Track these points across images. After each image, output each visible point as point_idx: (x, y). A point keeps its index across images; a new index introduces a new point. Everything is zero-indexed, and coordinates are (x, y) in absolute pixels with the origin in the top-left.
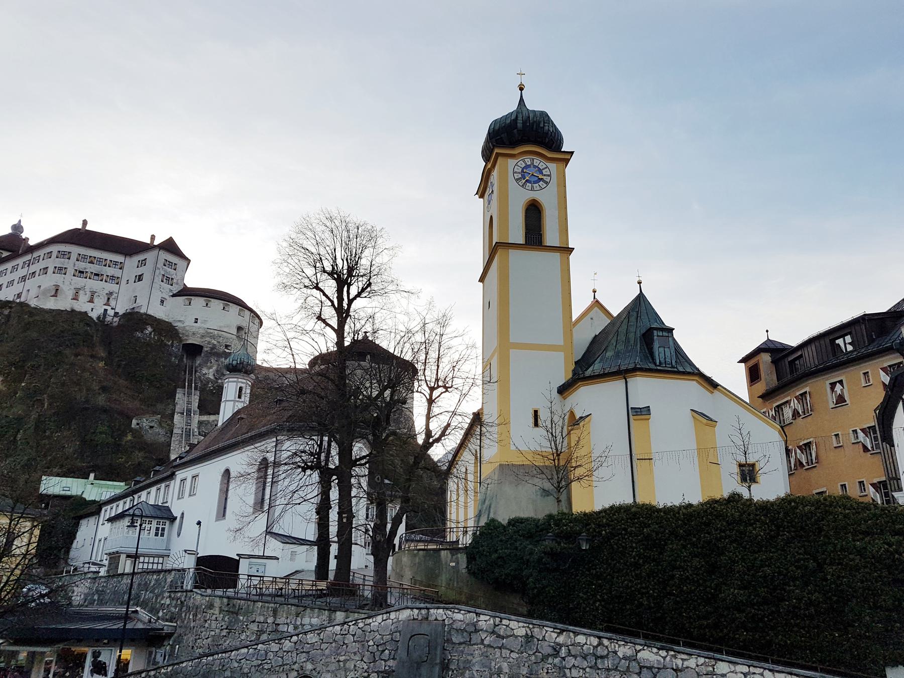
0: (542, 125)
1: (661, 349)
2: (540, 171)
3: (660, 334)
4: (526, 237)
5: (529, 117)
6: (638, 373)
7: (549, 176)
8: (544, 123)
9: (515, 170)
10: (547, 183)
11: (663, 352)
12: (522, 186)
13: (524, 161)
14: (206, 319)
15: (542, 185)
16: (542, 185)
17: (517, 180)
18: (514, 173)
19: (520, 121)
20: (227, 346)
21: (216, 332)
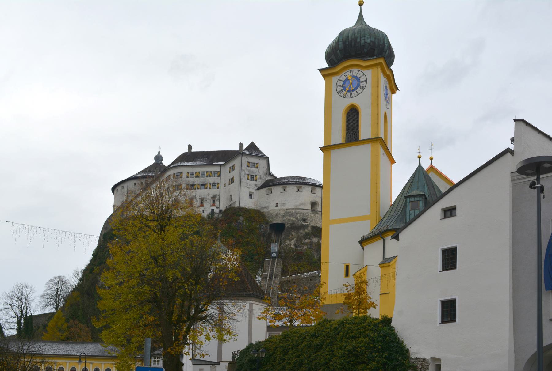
0: (358, 40)
1: (412, 212)
2: (357, 79)
3: (413, 199)
4: (346, 136)
5: (348, 37)
6: (389, 233)
7: (365, 81)
8: (361, 37)
9: (338, 84)
10: (363, 88)
11: (413, 214)
12: (343, 97)
13: (345, 75)
14: (284, 202)
15: (359, 90)
16: (359, 90)
17: (339, 93)
18: (337, 87)
19: (341, 43)
20: (304, 220)
21: (294, 211)
